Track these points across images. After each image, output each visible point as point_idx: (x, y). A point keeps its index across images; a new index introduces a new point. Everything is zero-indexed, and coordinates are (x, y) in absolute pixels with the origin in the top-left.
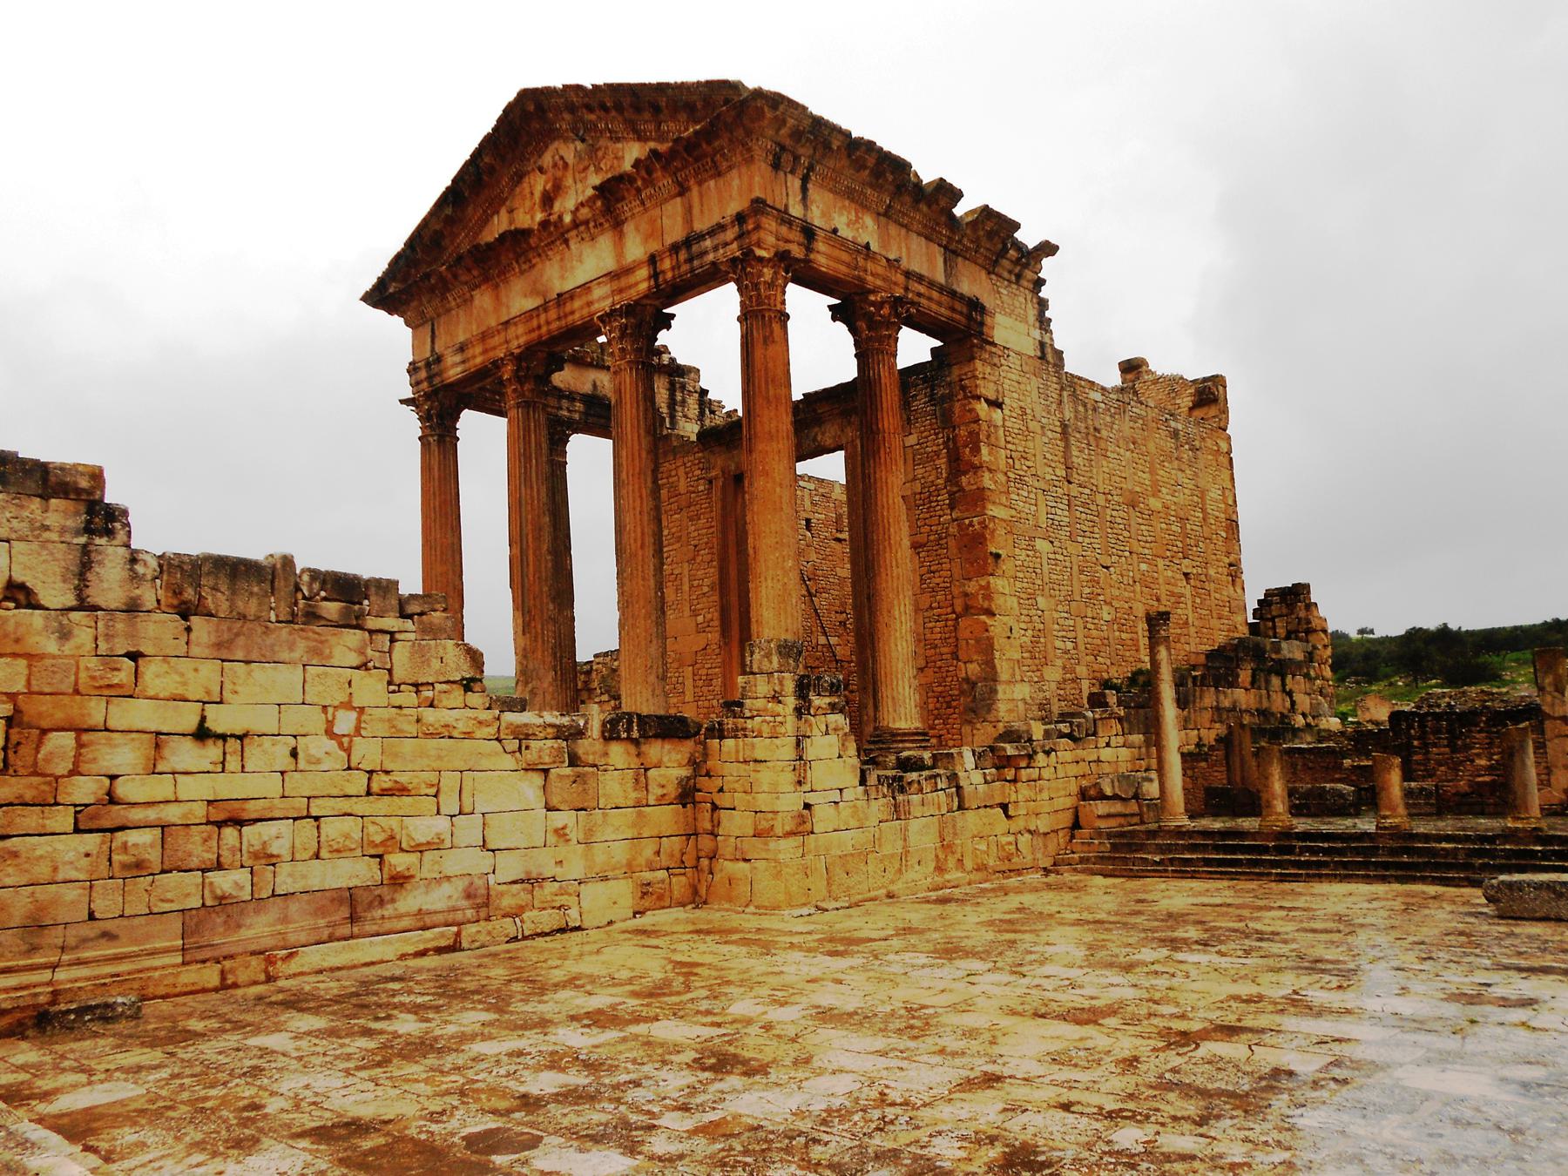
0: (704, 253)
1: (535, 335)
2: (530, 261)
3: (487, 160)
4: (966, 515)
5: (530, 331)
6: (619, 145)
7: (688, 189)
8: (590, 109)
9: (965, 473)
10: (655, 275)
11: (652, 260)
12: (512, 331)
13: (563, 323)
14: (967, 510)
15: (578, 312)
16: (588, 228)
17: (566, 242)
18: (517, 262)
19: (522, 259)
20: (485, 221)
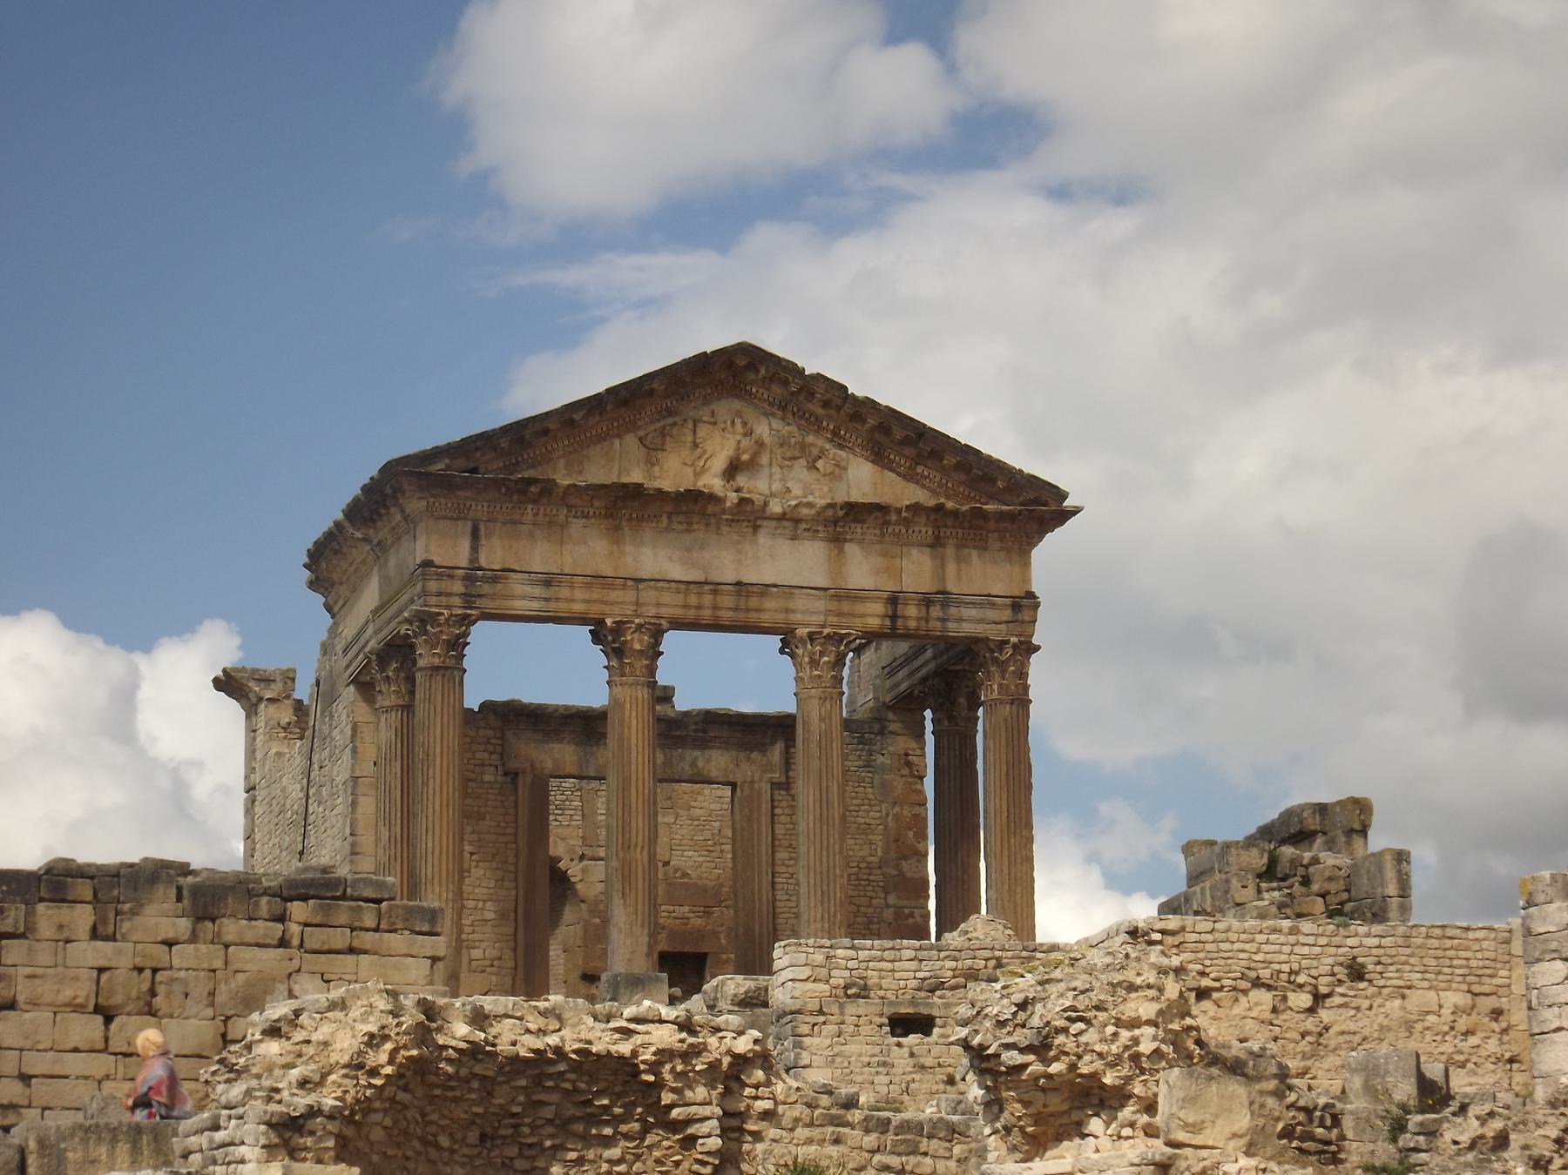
0: (960, 620)
1: (692, 612)
2: (690, 524)
3: (655, 385)
4: (903, 903)
5: (685, 606)
6: (843, 454)
7: (942, 545)
8: (826, 404)
9: (905, 858)
10: (894, 617)
11: (893, 600)
12: (648, 595)
13: (742, 616)
14: (908, 899)
15: (771, 611)
16: (795, 529)
17: (756, 528)
18: (669, 518)
19: (681, 518)
20: (601, 439)
